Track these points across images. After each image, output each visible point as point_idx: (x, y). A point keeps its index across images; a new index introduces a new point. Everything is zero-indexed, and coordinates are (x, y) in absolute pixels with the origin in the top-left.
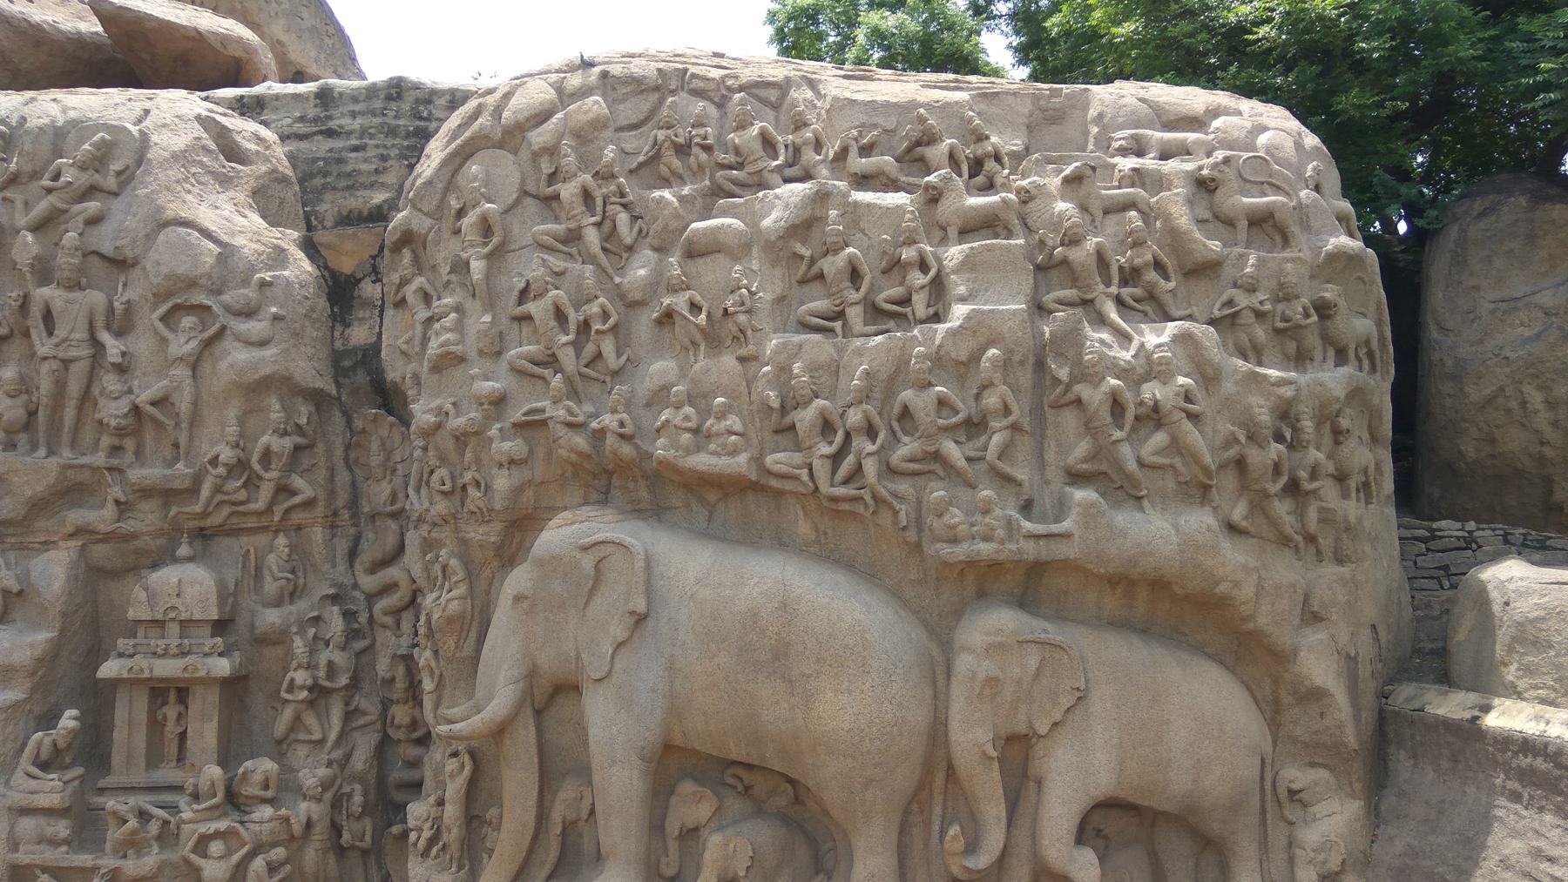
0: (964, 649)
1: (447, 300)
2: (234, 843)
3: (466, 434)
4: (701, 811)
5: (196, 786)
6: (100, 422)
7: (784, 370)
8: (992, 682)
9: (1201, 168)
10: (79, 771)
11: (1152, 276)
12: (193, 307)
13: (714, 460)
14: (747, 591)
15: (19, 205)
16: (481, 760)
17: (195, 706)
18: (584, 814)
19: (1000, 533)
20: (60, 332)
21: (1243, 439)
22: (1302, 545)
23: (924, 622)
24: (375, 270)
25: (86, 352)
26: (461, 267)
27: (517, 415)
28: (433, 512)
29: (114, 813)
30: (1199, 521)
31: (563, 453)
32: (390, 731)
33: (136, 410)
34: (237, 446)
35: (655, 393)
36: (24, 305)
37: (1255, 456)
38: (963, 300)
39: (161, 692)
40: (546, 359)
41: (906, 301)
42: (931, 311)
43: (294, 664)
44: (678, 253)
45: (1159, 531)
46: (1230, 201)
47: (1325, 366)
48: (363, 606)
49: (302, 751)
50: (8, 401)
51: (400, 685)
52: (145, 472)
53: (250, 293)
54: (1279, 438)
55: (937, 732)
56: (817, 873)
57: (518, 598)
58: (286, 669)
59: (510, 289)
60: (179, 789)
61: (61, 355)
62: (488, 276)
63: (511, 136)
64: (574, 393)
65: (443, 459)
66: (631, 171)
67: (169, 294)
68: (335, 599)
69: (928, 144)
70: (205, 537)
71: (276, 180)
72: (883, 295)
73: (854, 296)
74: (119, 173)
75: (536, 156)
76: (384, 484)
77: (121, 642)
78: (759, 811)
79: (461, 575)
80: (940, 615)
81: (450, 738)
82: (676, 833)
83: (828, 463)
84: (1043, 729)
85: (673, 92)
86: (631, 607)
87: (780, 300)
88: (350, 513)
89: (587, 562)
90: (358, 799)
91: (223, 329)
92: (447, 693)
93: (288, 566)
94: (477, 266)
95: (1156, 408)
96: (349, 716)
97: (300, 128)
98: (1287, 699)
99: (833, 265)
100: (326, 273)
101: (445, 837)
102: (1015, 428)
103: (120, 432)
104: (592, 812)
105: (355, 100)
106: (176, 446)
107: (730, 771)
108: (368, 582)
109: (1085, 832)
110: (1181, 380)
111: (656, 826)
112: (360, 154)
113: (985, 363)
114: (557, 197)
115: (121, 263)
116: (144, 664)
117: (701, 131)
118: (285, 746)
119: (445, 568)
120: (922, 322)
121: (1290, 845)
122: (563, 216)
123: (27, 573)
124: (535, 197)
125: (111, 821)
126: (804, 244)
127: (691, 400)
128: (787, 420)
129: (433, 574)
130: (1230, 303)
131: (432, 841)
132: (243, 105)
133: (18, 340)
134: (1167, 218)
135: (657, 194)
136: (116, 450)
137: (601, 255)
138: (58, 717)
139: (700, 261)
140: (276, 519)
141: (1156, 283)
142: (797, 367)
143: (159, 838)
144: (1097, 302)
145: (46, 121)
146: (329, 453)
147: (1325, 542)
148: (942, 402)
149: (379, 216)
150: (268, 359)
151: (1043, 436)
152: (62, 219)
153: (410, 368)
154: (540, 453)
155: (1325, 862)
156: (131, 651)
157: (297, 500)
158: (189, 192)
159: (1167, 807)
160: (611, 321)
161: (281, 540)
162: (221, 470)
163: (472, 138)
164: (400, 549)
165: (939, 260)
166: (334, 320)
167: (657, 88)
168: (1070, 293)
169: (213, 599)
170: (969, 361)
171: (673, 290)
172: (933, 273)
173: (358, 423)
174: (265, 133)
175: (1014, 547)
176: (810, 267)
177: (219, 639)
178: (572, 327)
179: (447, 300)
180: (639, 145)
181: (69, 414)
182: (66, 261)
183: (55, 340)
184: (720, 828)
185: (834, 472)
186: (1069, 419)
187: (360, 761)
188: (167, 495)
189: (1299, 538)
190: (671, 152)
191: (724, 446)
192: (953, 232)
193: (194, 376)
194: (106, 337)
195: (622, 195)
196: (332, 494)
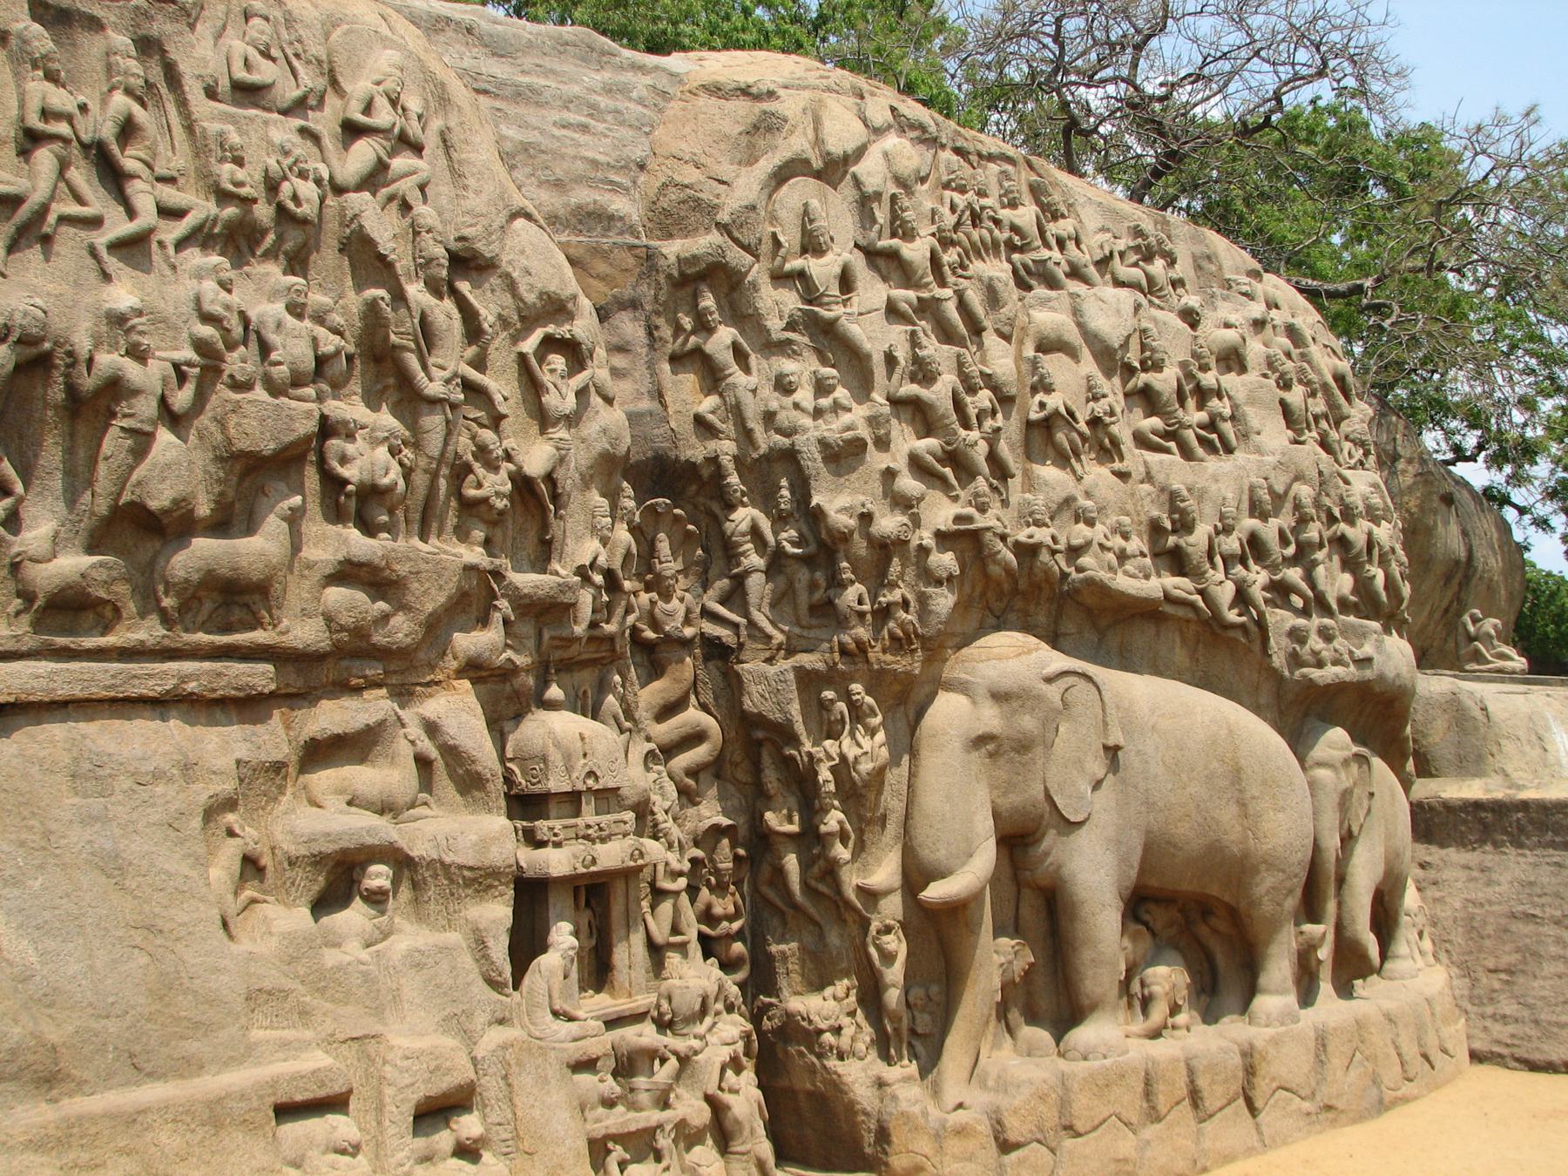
11: (1324, 424)
15: (327, 141)
17: (617, 910)
19: (1346, 657)
25: (462, 397)
31: (994, 570)
57: (980, 741)
63: (833, 169)
76: (675, 602)
79: (879, 718)
84: (1355, 829)
85: (943, 146)
86: (1111, 742)
99: (1165, 381)
114: (893, 255)
120: (1229, 450)
123: (432, 728)
136: (487, 543)
160: (999, 416)
162: (598, 579)
163: (792, 161)
167: (935, 140)
168: (1290, 433)
181: (443, 483)
183: (447, 374)
188: (545, 612)
195: (963, 267)
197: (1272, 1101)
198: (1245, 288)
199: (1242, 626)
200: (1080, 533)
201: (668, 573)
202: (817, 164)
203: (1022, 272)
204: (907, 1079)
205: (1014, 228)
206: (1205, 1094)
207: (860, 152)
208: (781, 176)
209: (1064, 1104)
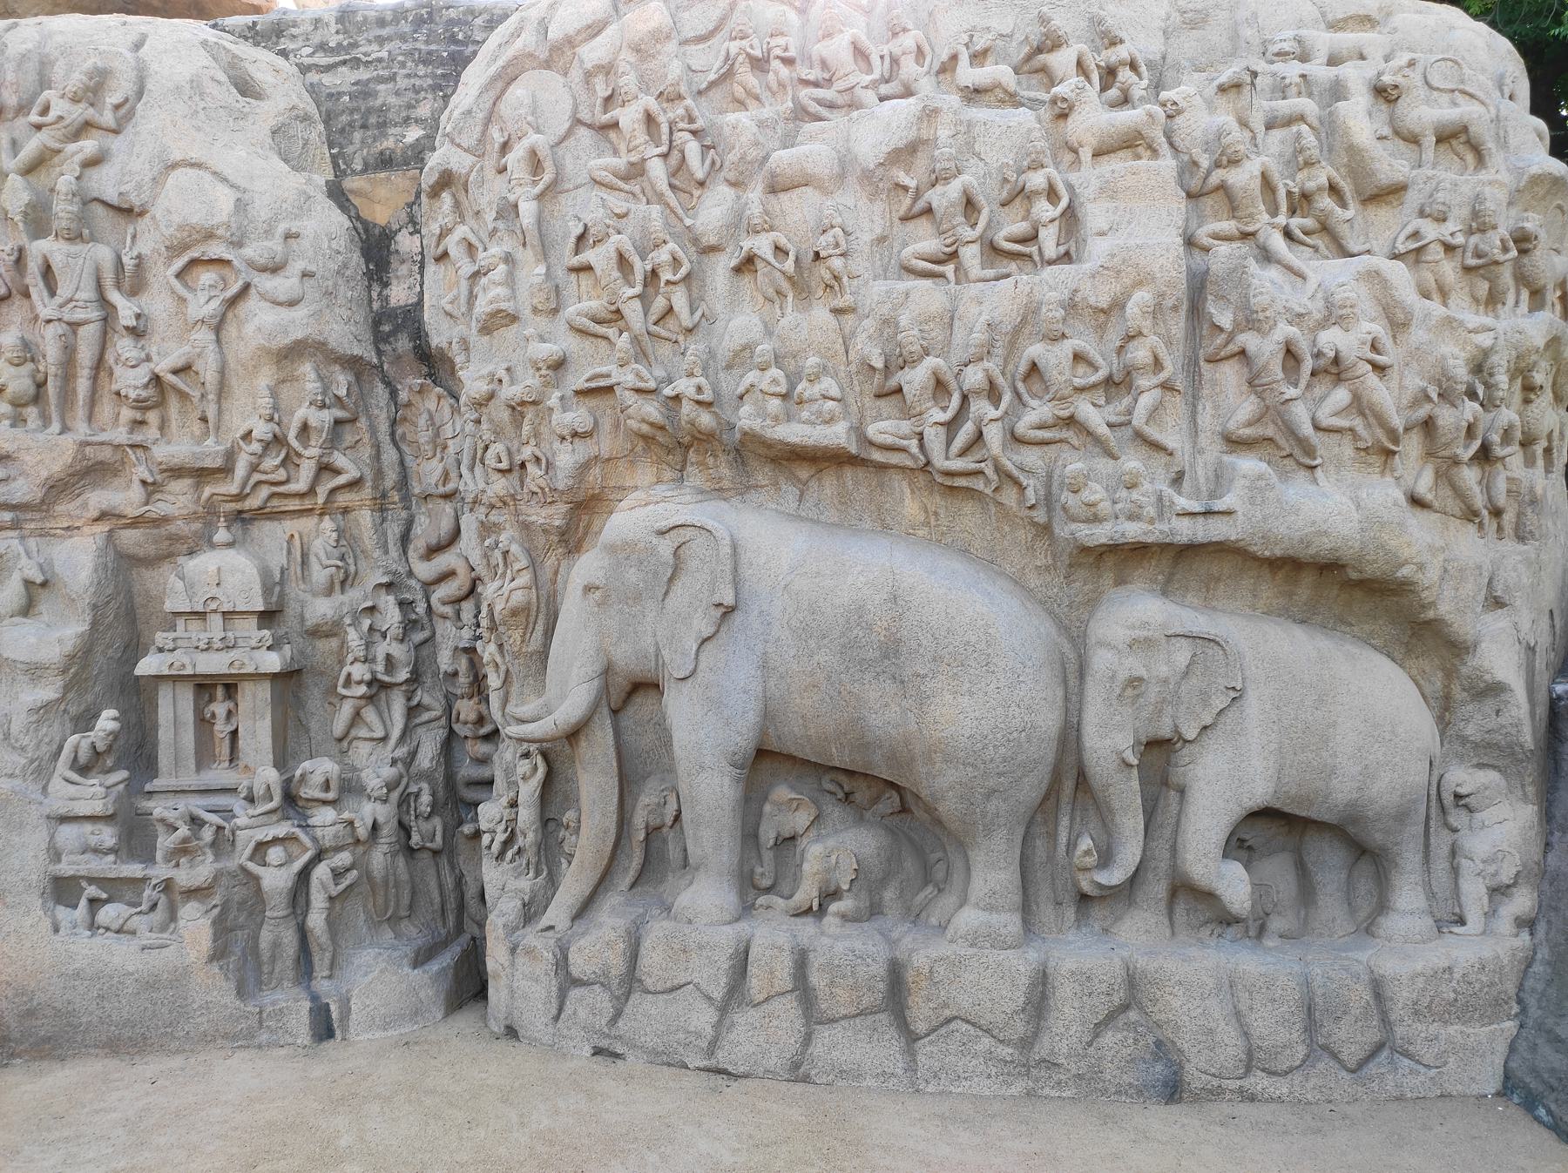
0: (1100, 644)
1: (495, 250)
2: (294, 848)
3: (523, 403)
4: (801, 819)
5: (250, 789)
6: (118, 394)
7: (888, 322)
8: (1135, 682)
9: (1380, 74)
10: (124, 774)
11: (1326, 202)
12: (212, 261)
13: (807, 429)
14: (850, 580)
16: (556, 757)
18: (669, 820)
19: (1150, 511)
20: (64, 291)
21: (1434, 396)
22: (1486, 521)
23: (1050, 613)
24: (412, 220)
25: (94, 314)
26: (509, 210)
27: (581, 384)
28: (490, 493)
29: (162, 820)
30: (1384, 493)
31: (632, 423)
32: (456, 727)
33: (156, 379)
34: (271, 419)
35: (736, 354)
36: (20, 260)
37: (1447, 417)
38: (1102, 234)
39: (204, 687)
40: (610, 316)
41: (1032, 238)
42: (1062, 249)
43: (350, 658)
44: (760, 187)
45: (1336, 506)
46: (1415, 114)
47: (1519, 311)
48: (419, 596)
49: (364, 749)
50: (13, 370)
51: (463, 680)
52: (171, 449)
53: (276, 245)
54: (1472, 395)
55: (1070, 737)
56: (926, 883)
57: (588, 589)
58: (341, 663)
59: (566, 236)
60: (232, 791)
61: (66, 317)
62: (539, 220)
63: (557, 55)
64: (641, 354)
65: (498, 433)
66: (700, 93)
67: (185, 247)
68: (389, 586)
69: (1051, 50)
70: (243, 520)
71: (297, 117)
72: (1003, 233)
73: (969, 234)
74: (117, 107)
75: (588, 76)
76: (435, 462)
77: (161, 638)
78: (860, 820)
79: (524, 563)
80: (1070, 606)
81: (521, 740)
82: (771, 842)
83: (942, 430)
84: (1190, 734)
86: (717, 599)
87: (881, 240)
88: (397, 494)
89: (665, 547)
90: (426, 798)
91: (246, 287)
92: (515, 689)
93: (336, 553)
94: (528, 210)
95: (1336, 360)
96: (412, 711)
97: (322, 60)
98: (1458, 694)
99: (945, 197)
100: (359, 225)
101: (520, 841)
102: (1166, 387)
103: (141, 405)
104: (677, 817)
105: (381, 23)
106: (204, 419)
107: (827, 777)
108: (425, 570)
109: (1238, 845)
110: (1366, 326)
111: (750, 836)
112: (390, 86)
113: (1132, 309)
114: (615, 125)
115: (127, 212)
116: (186, 660)
117: (781, 41)
118: (345, 744)
119: (506, 553)
120: (1051, 263)
121: (1453, 853)
122: (623, 147)
124: (589, 126)
125: (160, 829)
126: (907, 172)
127: (778, 360)
128: (892, 383)
129: (493, 562)
130: (1415, 235)
131: (507, 843)
132: (257, 33)
133: (17, 300)
134: (1346, 133)
135: (731, 117)
137: (668, 193)
138: (96, 716)
139: (782, 196)
140: (321, 500)
141: (1332, 212)
142: (904, 321)
143: (213, 844)
144: (1261, 237)
145: (30, 46)
146: (373, 430)
147: (1509, 518)
148: (1078, 357)
149: (417, 155)
150: (298, 324)
151: (1196, 397)
152: (56, 160)
153: (459, 330)
154: (606, 425)
155: (1495, 875)
156: (171, 646)
157: (341, 480)
158: (198, 129)
159: (1326, 817)
161: (328, 524)
162: (256, 447)
164: (457, 533)
165: (1070, 188)
166: (371, 279)
168: (1228, 226)
169: (257, 589)
170: (1111, 308)
171: (754, 231)
172: (1064, 203)
173: (403, 396)
174: (280, 61)
175: (1165, 527)
176: (916, 199)
177: (266, 633)
178: (639, 277)
179: (495, 250)
180: (708, 60)
181: (83, 385)
182: (63, 210)
183: (58, 300)
184: (819, 838)
185: (949, 443)
186: (1230, 374)
187: (427, 756)
188: (201, 475)
189: (1485, 513)
190: (747, 67)
191: (819, 413)
192: (1086, 154)
193: (218, 341)
194: (115, 297)
195: (691, 120)
196: (379, 474)
197: (943, 1031)
198: (1286, 47)
199: (981, 472)
200: (751, 377)
201: (422, 441)
202: (543, 55)
203: (814, 108)
204: (518, 891)
205: (824, 65)
206: (821, 995)
207: (594, 30)
208: (506, 77)
209: (633, 957)
